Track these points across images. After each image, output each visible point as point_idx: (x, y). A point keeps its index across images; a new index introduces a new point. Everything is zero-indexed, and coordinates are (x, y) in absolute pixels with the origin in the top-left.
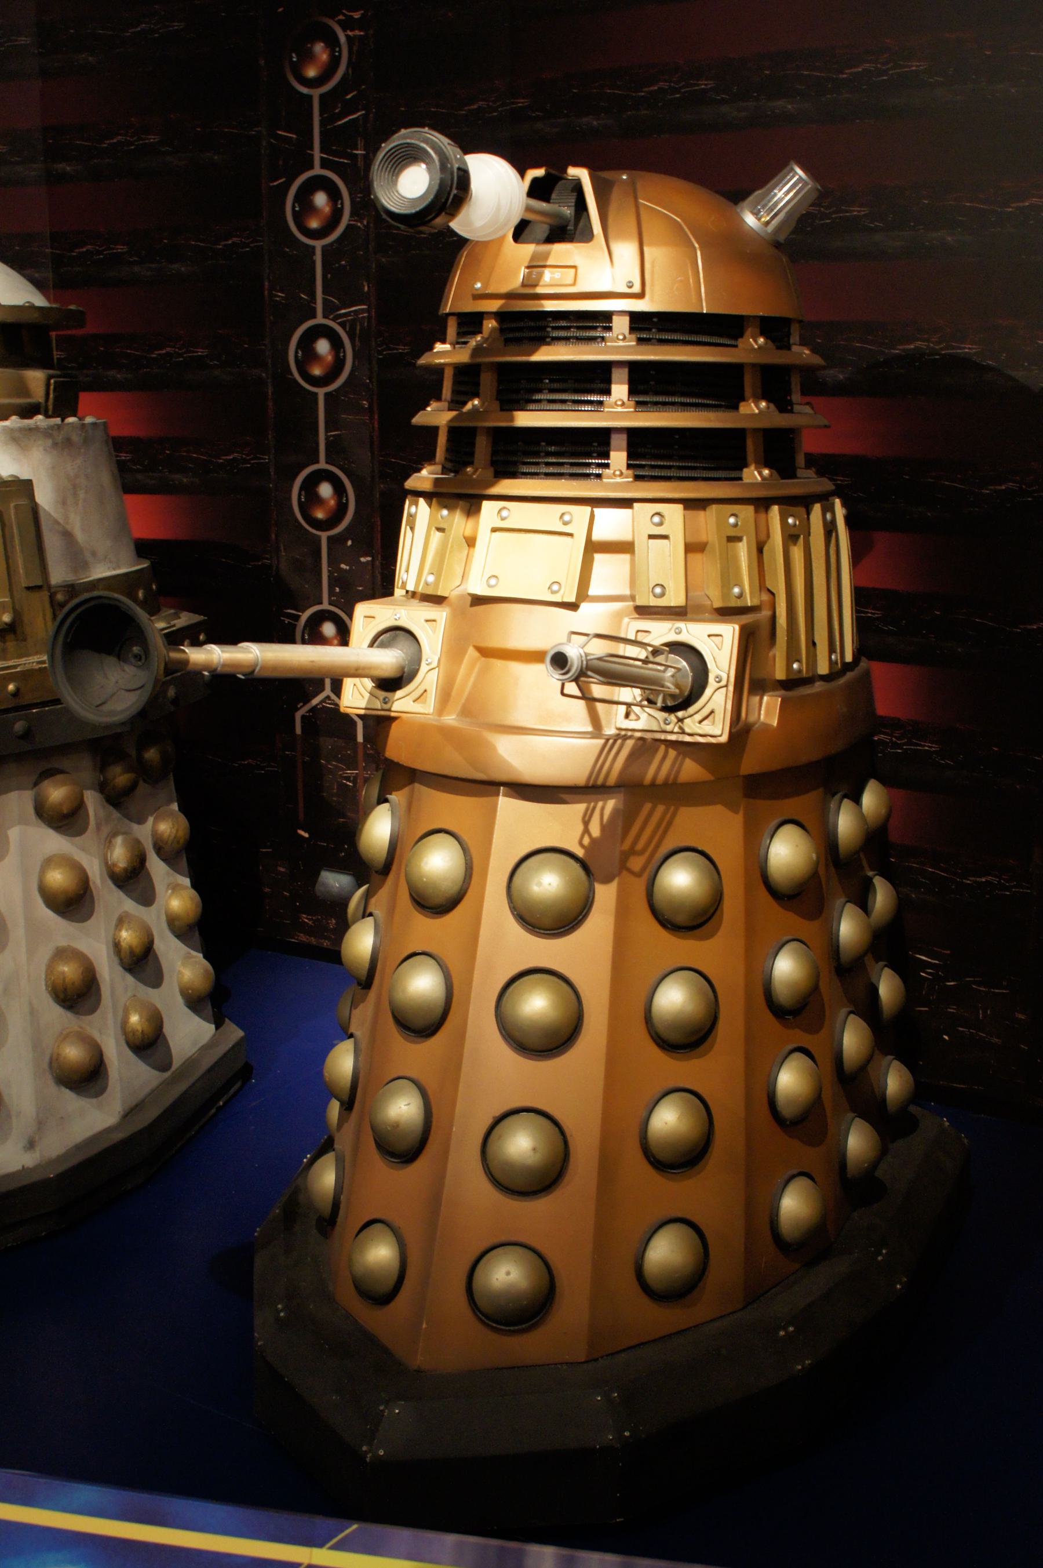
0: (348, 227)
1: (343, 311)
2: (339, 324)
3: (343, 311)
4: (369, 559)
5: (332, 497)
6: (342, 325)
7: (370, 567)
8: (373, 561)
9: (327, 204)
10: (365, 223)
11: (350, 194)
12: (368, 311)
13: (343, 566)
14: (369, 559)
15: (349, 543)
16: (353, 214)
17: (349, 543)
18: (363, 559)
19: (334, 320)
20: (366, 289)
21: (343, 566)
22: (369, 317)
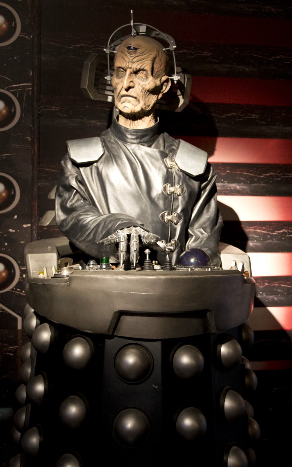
0: (19, 38)
1: (15, 86)
2: (11, 92)
3: (15, 86)
4: (29, 225)
5: (4, 191)
6: (14, 93)
7: (29, 230)
8: (31, 226)
9: (5, 23)
10: (31, 37)
11: (21, 19)
12: (32, 86)
13: (11, 230)
14: (29, 225)
15: (16, 217)
16: (22, 31)
17: (16, 217)
18: (25, 226)
19: (7, 90)
20: (31, 74)
21: (11, 230)
22: (33, 91)
